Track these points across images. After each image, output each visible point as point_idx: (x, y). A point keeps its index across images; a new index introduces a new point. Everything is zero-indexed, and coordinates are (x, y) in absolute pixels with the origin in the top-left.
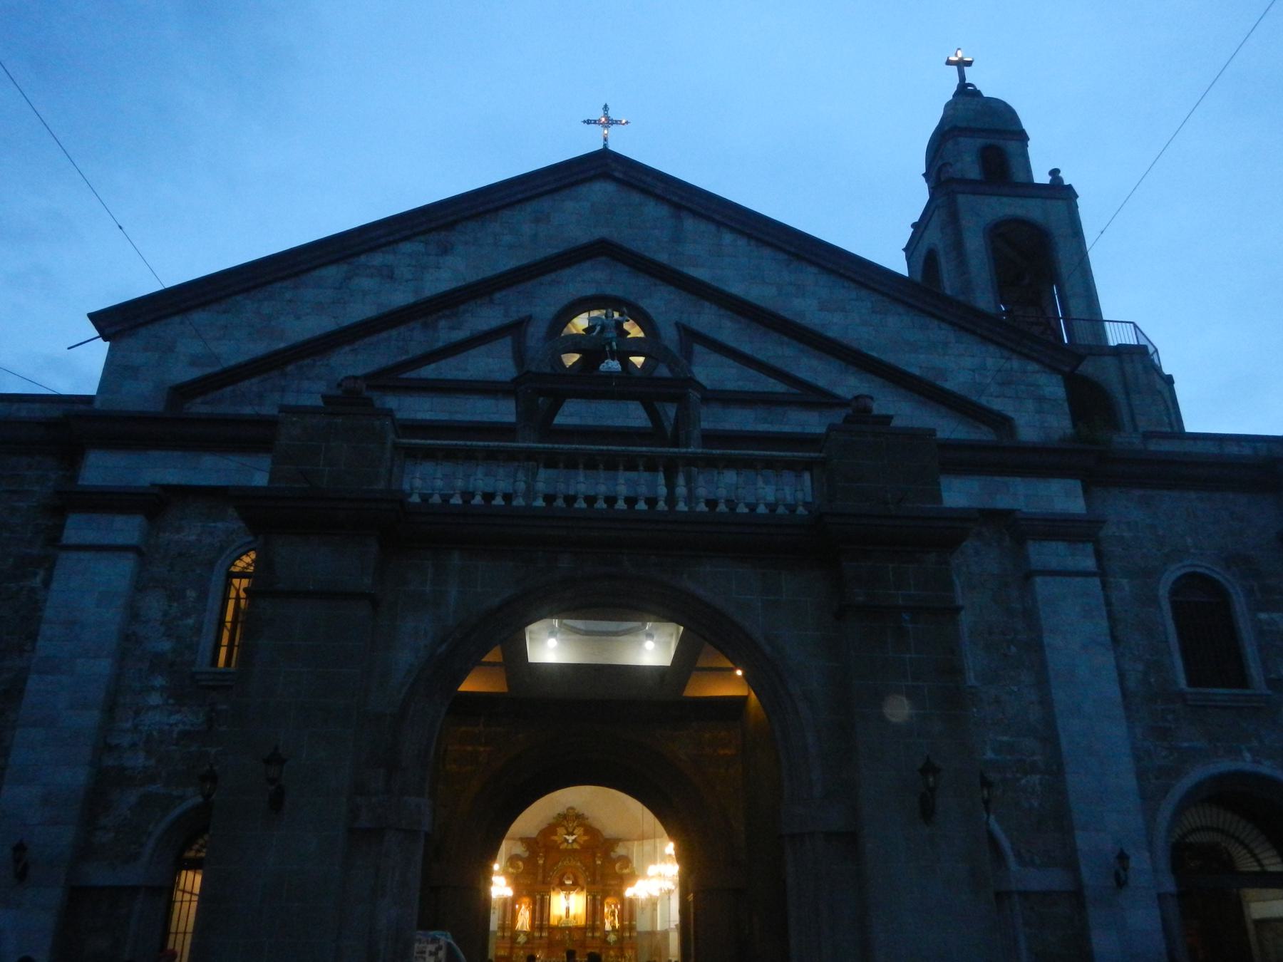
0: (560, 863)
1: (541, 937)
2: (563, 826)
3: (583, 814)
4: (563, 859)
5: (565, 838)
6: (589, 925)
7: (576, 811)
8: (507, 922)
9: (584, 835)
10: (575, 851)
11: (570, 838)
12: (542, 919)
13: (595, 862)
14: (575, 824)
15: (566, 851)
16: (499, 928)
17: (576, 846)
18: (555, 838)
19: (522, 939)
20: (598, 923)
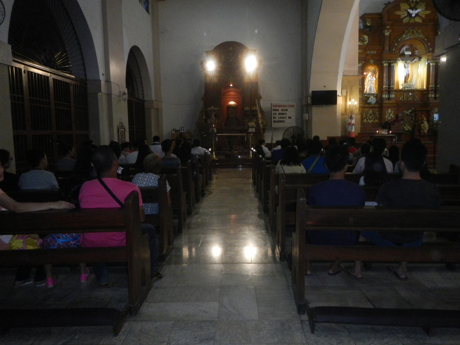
0: (404, 36)
1: (389, 99)
4: (406, 31)
5: (408, 13)
6: (432, 87)
9: (426, 9)
10: (416, 24)
11: (414, 13)
12: (389, 85)
15: (408, 25)
17: (418, 20)
18: (398, 13)
19: (372, 100)
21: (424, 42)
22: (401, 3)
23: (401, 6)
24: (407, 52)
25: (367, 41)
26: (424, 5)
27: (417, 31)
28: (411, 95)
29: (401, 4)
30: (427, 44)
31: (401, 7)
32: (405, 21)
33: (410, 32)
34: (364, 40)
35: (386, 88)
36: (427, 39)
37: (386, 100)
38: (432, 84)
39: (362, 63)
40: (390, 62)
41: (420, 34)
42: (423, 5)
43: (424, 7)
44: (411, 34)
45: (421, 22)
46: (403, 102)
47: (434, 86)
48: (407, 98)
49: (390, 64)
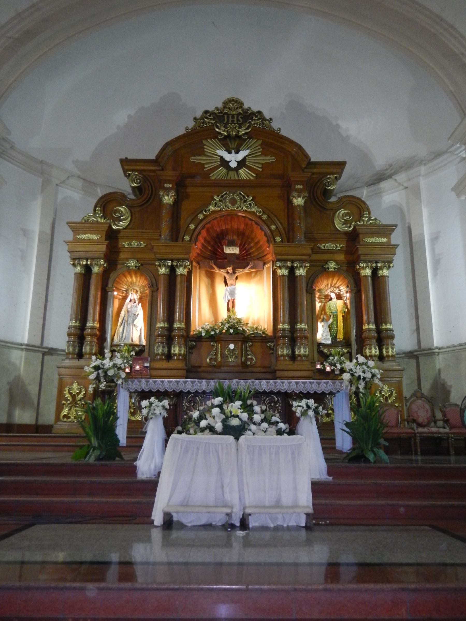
0: (212, 208)
2: (215, 135)
3: (259, 112)
5: (222, 158)
7: (246, 106)
8: (90, 324)
9: (264, 154)
12: (170, 318)
13: (290, 203)
14: (242, 132)
16: (69, 335)
20: (303, 326)
21: (262, 223)
22: (206, 139)
23: (205, 145)
24: (230, 248)
25: (129, 219)
26: (259, 145)
27: (244, 197)
28: (233, 350)
29: (204, 142)
31: (205, 148)
32: (213, 176)
33: (225, 199)
34: (120, 217)
35: (163, 328)
36: (268, 216)
37: (161, 359)
38: (283, 323)
39: (100, 266)
40: (170, 263)
41: (250, 204)
42: (256, 145)
43: (259, 149)
44: (230, 205)
45: (252, 178)
46: (214, 366)
47: (286, 326)
48: (223, 356)
49: (172, 269)
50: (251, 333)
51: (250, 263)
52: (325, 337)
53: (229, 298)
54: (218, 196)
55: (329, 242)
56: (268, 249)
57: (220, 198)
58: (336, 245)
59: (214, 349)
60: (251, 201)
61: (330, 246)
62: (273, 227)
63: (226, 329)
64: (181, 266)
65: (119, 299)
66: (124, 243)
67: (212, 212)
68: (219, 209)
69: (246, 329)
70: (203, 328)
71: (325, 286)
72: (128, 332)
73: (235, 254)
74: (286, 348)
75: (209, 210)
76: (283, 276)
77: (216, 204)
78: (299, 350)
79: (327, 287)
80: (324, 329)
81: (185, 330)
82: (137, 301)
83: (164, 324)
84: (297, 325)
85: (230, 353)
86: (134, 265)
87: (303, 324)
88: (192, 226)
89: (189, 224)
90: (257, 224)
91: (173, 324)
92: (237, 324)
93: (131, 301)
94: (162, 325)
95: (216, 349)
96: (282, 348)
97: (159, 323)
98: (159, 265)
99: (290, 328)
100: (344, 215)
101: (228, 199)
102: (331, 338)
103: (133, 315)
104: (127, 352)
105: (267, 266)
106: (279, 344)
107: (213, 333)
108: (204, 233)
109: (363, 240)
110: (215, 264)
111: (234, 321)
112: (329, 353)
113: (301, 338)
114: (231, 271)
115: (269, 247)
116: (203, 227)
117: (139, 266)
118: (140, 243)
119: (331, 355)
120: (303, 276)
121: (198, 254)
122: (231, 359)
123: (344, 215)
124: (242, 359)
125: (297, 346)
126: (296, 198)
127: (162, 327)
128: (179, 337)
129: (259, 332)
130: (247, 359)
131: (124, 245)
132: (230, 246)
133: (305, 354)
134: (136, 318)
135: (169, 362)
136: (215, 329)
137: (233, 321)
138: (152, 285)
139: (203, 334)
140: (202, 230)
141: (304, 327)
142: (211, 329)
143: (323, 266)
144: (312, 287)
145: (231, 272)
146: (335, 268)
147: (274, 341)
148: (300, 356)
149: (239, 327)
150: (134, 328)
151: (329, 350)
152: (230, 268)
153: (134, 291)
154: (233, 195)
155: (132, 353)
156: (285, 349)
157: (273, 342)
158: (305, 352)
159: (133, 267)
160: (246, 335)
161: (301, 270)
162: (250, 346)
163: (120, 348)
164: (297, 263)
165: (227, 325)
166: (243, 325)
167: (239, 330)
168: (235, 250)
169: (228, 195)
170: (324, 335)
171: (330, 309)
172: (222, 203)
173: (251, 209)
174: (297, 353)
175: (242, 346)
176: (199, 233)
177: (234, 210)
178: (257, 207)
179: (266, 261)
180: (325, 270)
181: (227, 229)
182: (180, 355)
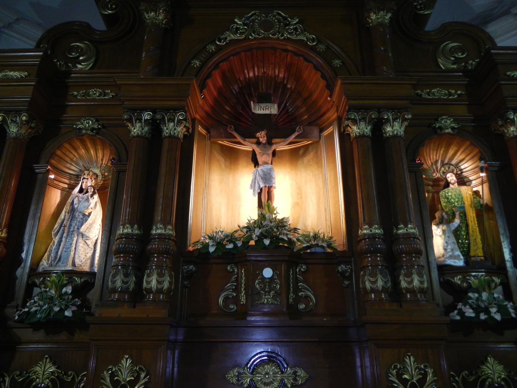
24: (263, 105)
28: (271, 279)
30: (330, 64)
33: (253, 21)
34: (79, 57)
35: (127, 236)
47: (377, 230)
50: (305, 245)
51: (297, 128)
52: (451, 253)
53: (262, 185)
54: (240, 19)
55: (435, 86)
56: (329, 99)
57: (245, 20)
58: (449, 92)
59: (233, 278)
60: (295, 24)
61: (438, 93)
62: (337, 62)
63: (257, 239)
64: (171, 120)
65: (63, 190)
66: (76, 93)
67: (230, 40)
68: (243, 36)
69: (295, 240)
70: (210, 238)
71: (432, 163)
72: (68, 249)
73: (269, 115)
74: (381, 274)
75: (226, 38)
76: (361, 137)
77: (237, 29)
78: (409, 279)
79: (436, 165)
80: (447, 238)
81: (173, 240)
82: (91, 190)
83: (132, 227)
84: (398, 229)
85: (265, 286)
86: (89, 126)
87: (409, 226)
88: (197, 63)
89: (192, 59)
90: (306, 59)
91: (151, 229)
92: (277, 229)
93: (81, 191)
94: (128, 230)
95: (237, 278)
96: (373, 275)
97: (121, 227)
98: (130, 120)
99: (384, 234)
100: (453, 50)
101: (257, 23)
102: (463, 255)
103: (81, 216)
104: (54, 287)
105: (326, 133)
106: (364, 267)
107: (231, 246)
108: (217, 75)
109: (506, 74)
110: (236, 130)
111: (272, 224)
112: (465, 285)
113: (409, 254)
114: (263, 140)
115: (331, 96)
116: (216, 66)
117: (99, 129)
118: (105, 92)
119: (470, 288)
120: (400, 136)
121: (206, 112)
122: (267, 299)
123: (453, 50)
124: (288, 299)
125: (403, 272)
126: (375, 13)
127: (127, 234)
128: (160, 253)
129: (320, 244)
130: (298, 300)
131: (76, 96)
132: (262, 103)
133: (422, 286)
134: (86, 220)
135: (134, 307)
136: (236, 239)
137: (270, 224)
138: (120, 160)
139: (212, 249)
140: (214, 71)
141: (412, 231)
142: (226, 239)
143: (430, 126)
144: (415, 161)
145: (264, 142)
146: (453, 128)
147: (351, 262)
148: (411, 291)
149: (280, 234)
150: (80, 240)
151: (464, 280)
152: (263, 133)
153: (88, 175)
154: (266, 17)
155: (64, 290)
156: (379, 277)
157: (347, 263)
158: (422, 282)
159: (87, 130)
160: (295, 250)
161: (397, 126)
162: (302, 272)
163: (44, 278)
164: (389, 114)
165: (258, 232)
166: (289, 231)
167: (282, 239)
168: (272, 109)
169: (258, 17)
170: (449, 250)
171: (449, 202)
172: (248, 27)
173: (297, 35)
174: (404, 284)
175: (288, 272)
176: (209, 76)
177: (269, 38)
178: (308, 33)
179: (325, 125)
180: (436, 133)
181: (256, 78)
182: (159, 291)
